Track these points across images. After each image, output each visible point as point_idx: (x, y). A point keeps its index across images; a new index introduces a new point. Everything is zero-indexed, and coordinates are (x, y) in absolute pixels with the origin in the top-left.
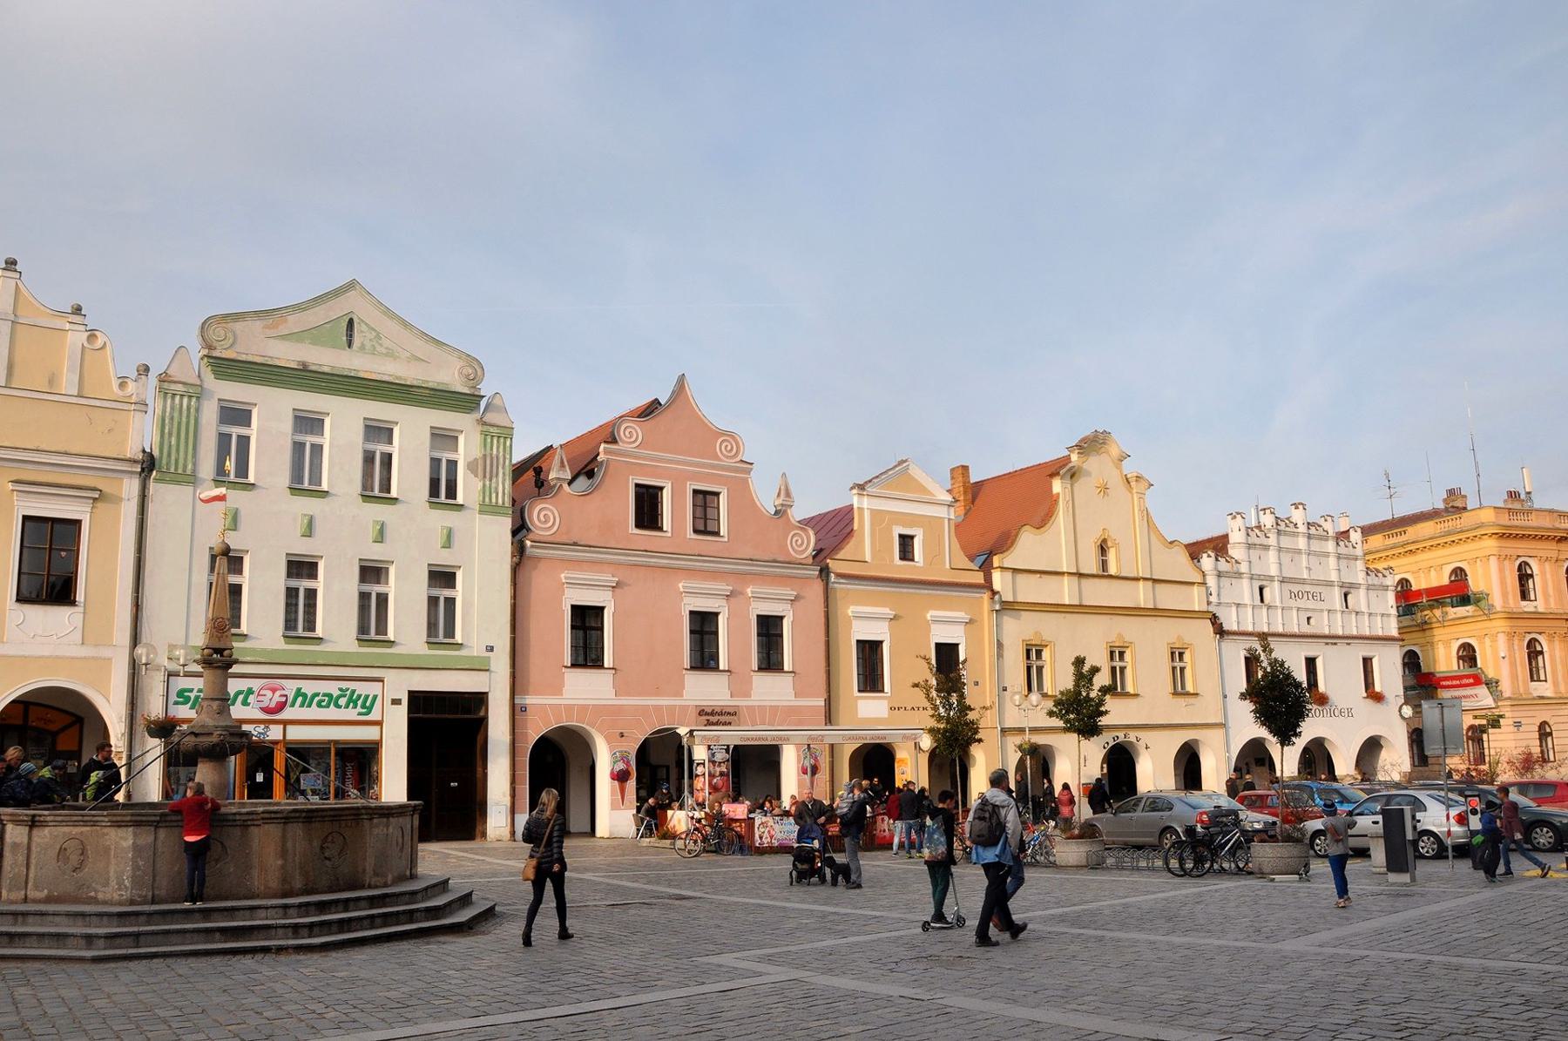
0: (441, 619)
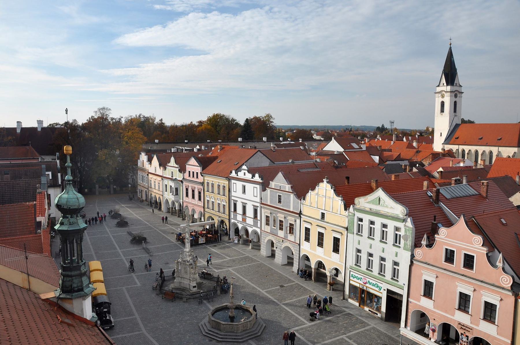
0: (395, 274)
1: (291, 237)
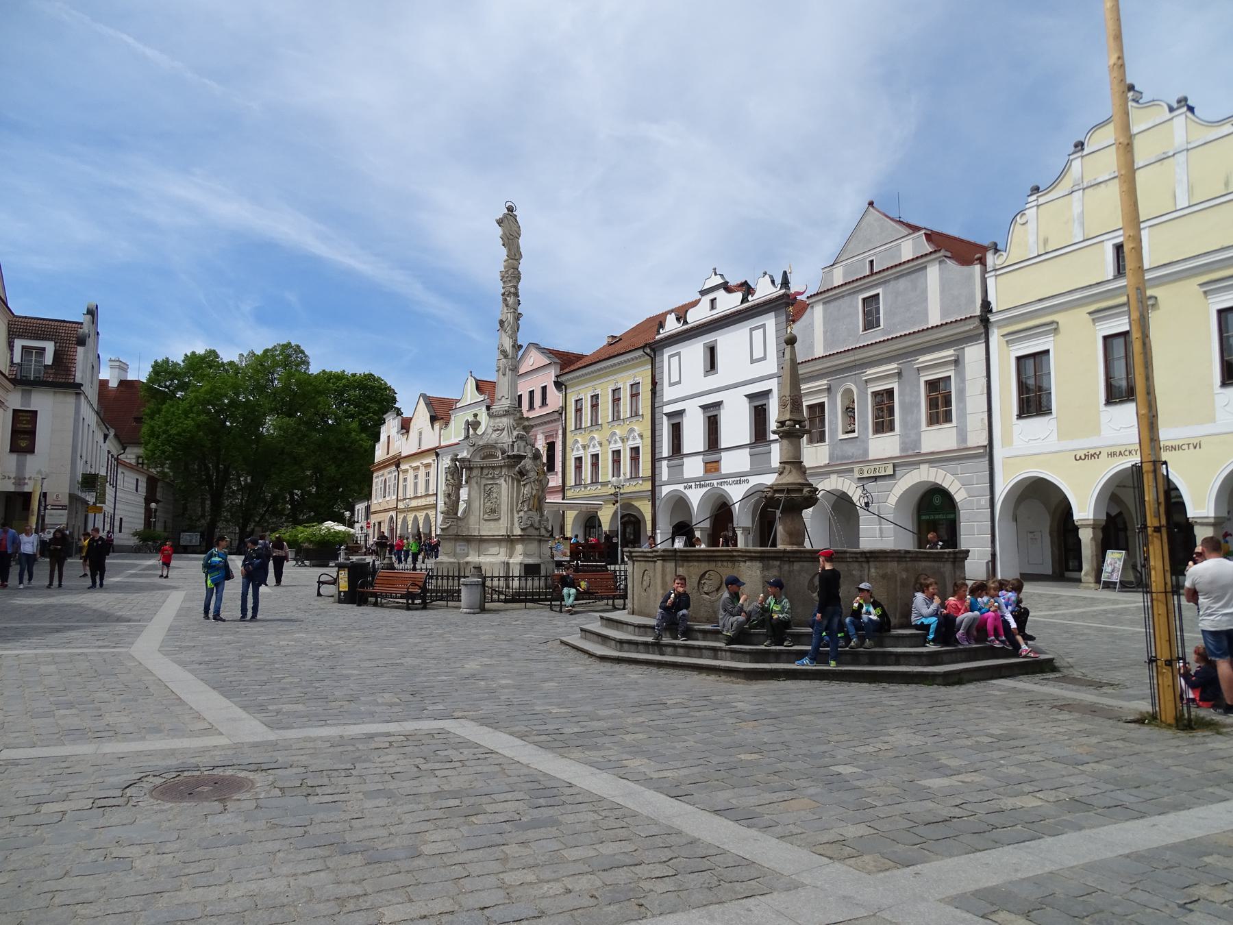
1: (938, 439)
